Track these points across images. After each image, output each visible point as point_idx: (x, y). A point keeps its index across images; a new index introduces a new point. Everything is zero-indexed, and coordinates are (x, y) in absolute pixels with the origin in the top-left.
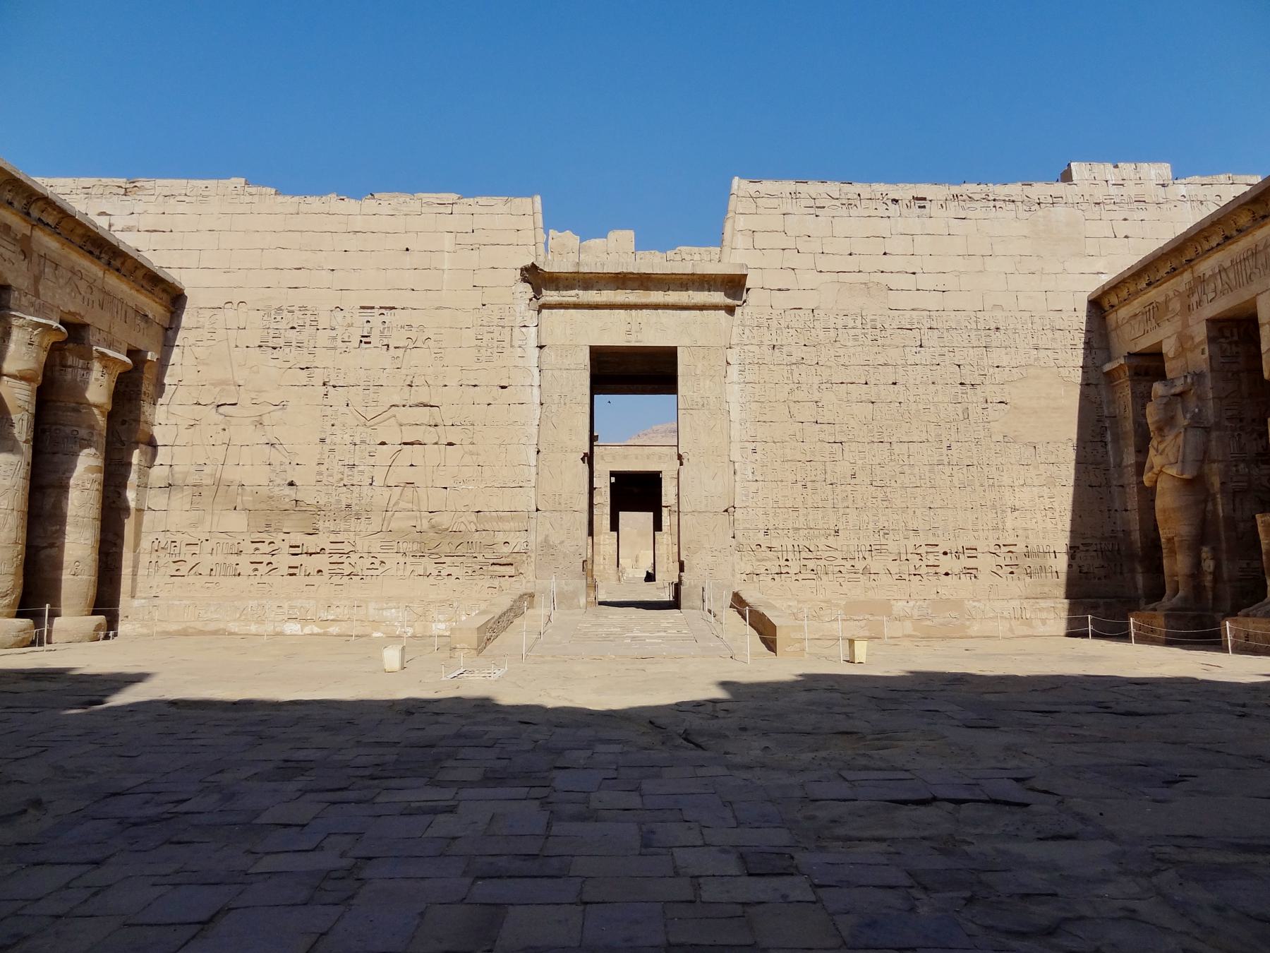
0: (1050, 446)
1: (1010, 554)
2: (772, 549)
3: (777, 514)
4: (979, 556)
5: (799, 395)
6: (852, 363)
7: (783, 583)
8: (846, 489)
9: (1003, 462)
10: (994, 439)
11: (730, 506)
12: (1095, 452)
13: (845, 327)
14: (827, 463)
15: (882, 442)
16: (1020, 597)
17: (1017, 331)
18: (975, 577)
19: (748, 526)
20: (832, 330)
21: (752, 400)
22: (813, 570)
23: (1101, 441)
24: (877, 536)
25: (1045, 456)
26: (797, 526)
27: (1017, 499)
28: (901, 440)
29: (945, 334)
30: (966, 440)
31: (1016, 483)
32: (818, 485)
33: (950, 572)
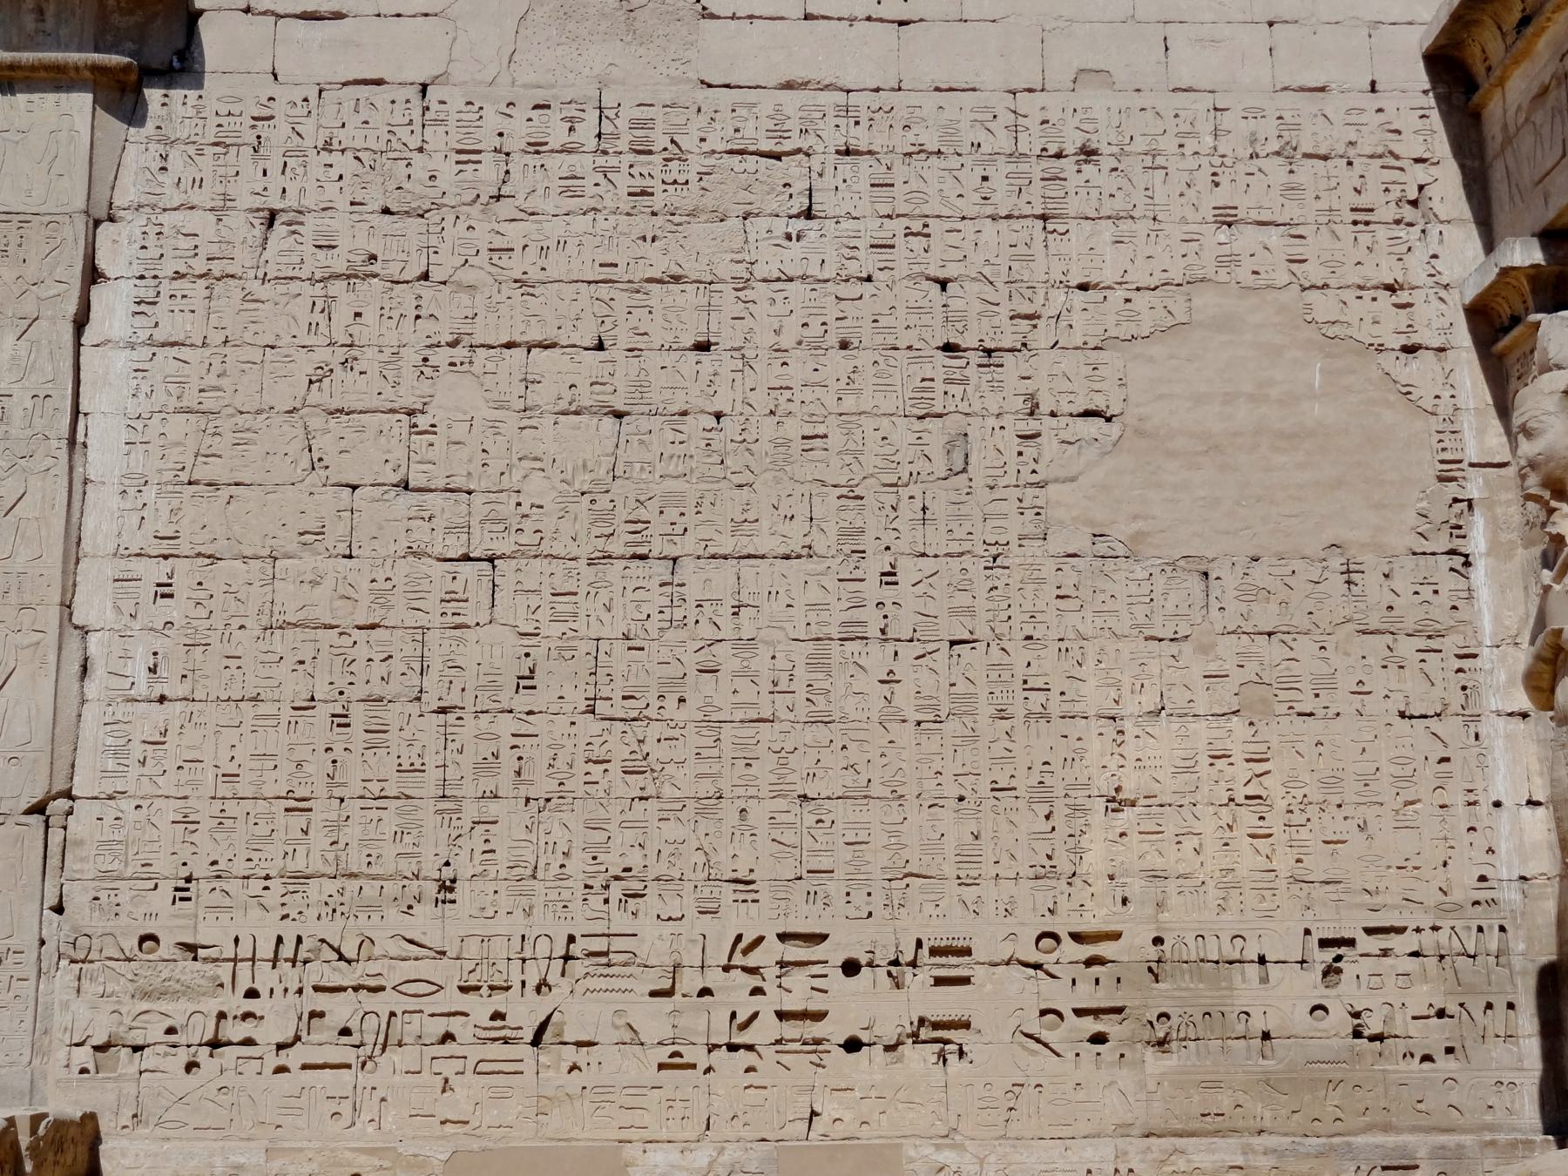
0: (1259, 574)
1: (1096, 969)
2: (200, 951)
3: (228, 823)
4: (979, 973)
5: (346, 389)
6: (552, 273)
7: (229, 1079)
8: (494, 729)
9: (1087, 629)
10: (1057, 544)
11: (53, 792)
12: (1426, 591)
13: (536, 147)
14: (429, 636)
15: (643, 557)
16: (1123, 1130)
17: (1160, 161)
18: (961, 1053)
19: (116, 866)
20: (487, 158)
21: (173, 403)
22: (345, 1032)
23: (1452, 552)
24: (596, 901)
25: (1244, 608)
26: (299, 864)
27: (1130, 763)
28: (712, 550)
29: (900, 172)
30: (955, 548)
31: (1130, 707)
32: (392, 715)
33: (865, 1037)
